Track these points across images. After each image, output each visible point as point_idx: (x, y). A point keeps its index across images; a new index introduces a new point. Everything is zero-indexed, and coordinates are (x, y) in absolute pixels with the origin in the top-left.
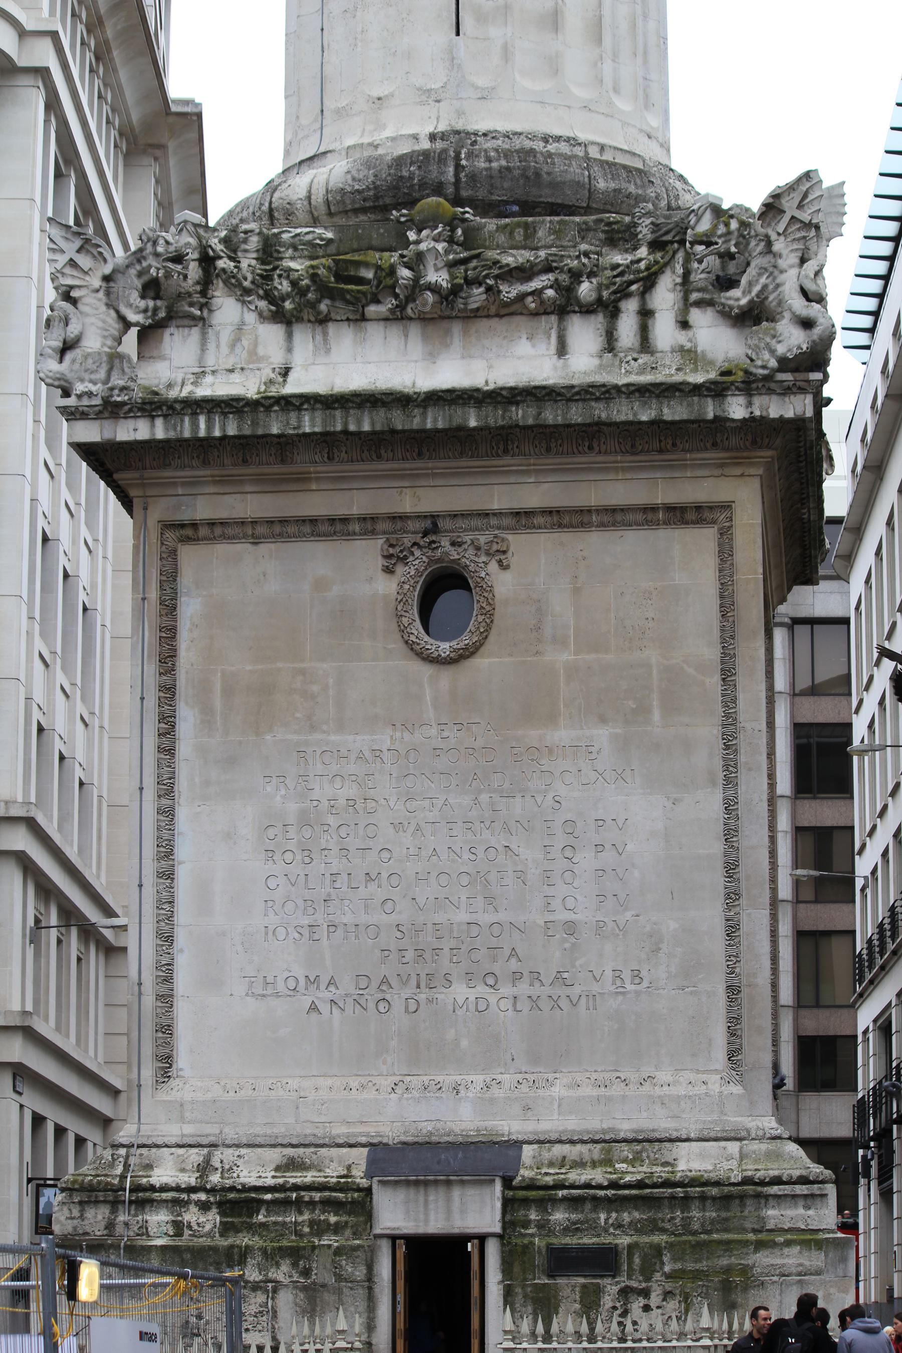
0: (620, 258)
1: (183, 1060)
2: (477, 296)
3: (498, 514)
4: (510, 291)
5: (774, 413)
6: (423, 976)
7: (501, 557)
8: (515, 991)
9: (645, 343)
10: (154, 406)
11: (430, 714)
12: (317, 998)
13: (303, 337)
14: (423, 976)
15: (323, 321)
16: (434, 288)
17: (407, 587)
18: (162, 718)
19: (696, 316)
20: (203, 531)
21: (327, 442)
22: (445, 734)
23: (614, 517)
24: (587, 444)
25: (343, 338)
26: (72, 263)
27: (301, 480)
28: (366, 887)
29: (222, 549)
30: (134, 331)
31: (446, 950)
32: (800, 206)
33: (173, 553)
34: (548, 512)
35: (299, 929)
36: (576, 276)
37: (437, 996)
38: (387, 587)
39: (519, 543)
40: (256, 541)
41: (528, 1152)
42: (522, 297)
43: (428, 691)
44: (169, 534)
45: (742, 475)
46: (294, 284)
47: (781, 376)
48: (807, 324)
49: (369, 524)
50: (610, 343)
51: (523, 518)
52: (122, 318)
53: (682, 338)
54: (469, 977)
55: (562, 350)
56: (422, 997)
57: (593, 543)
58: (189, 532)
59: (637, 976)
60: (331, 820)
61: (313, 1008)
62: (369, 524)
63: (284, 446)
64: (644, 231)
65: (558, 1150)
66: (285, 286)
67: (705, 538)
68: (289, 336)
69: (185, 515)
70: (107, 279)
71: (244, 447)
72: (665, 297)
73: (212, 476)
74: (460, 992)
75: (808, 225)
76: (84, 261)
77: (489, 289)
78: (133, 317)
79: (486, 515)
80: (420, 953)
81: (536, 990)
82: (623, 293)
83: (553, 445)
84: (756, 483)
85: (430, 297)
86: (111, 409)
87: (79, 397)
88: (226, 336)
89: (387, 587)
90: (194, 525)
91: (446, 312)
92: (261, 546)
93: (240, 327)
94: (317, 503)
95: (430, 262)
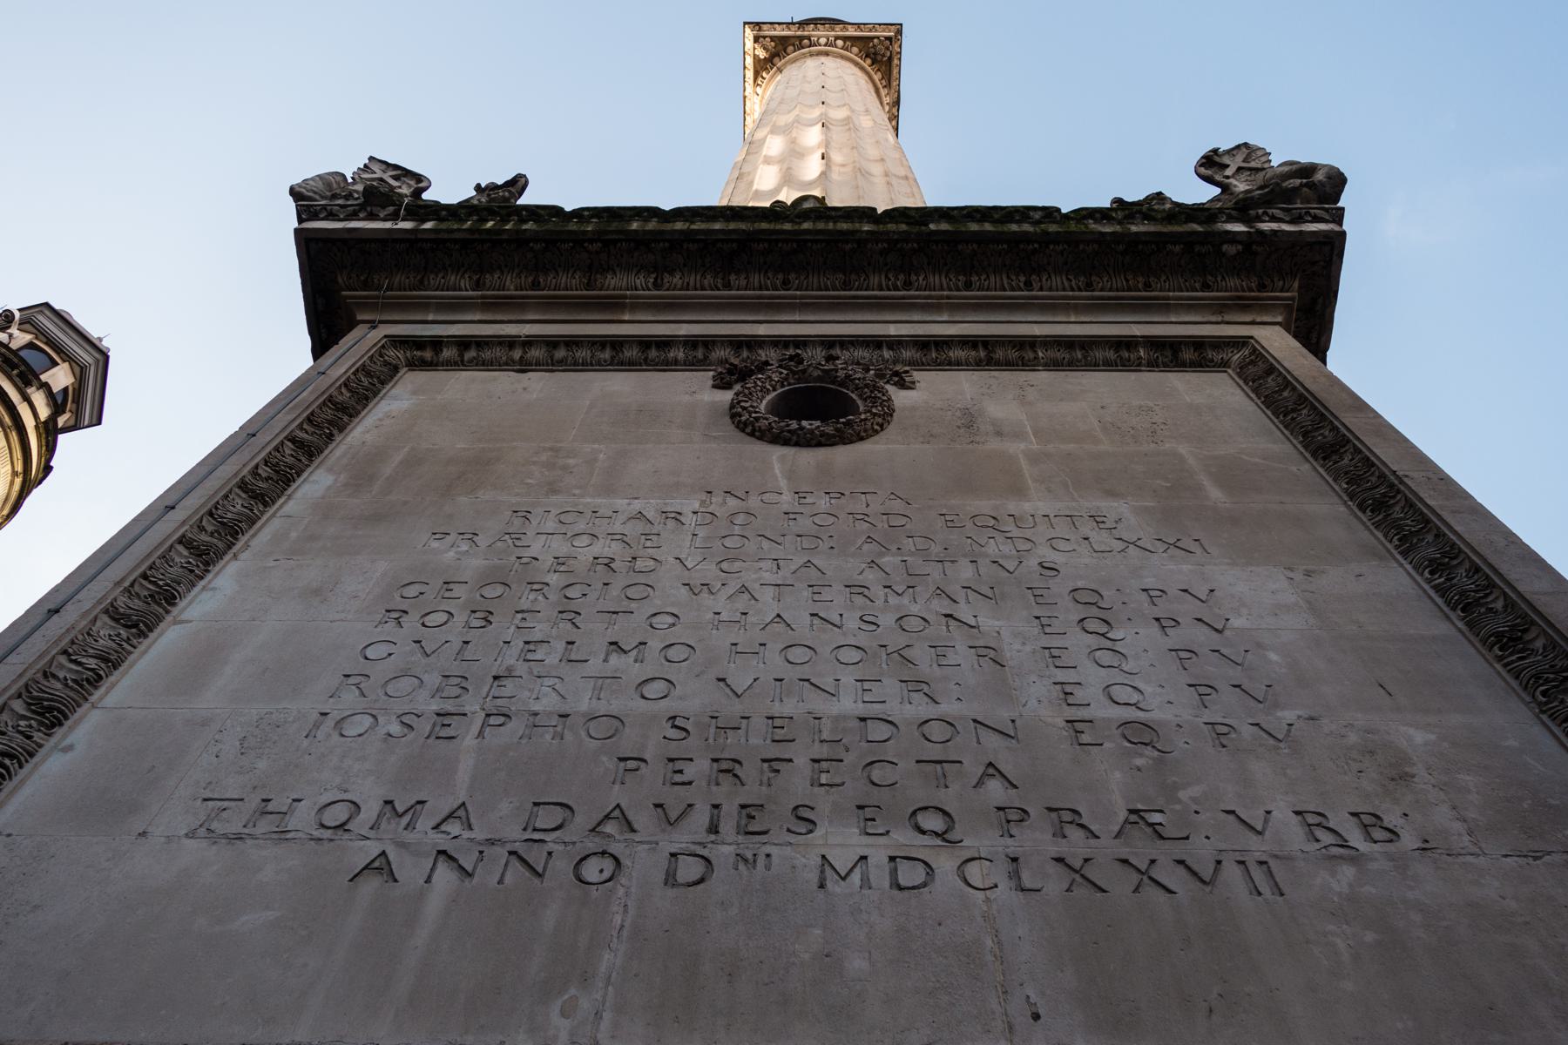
3: (895, 343)
6: (730, 809)
8: (1012, 846)
11: (783, 483)
12: (402, 845)
14: (730, 809)
20: (447, 353)
23: (1075, 354)
24: (1023, 279)
27: (613, 305)
28: (605, 660)
31: (801, 761)
35: (406, 719)
37: (768, 849)
44: (392, 354)
54: (867, 814)
56: (723, 852)
58: (428, 355)
59: (1370, 823)
60: (553, 579)
61: (381, 867)
62: (697, 353)
73: (483, 297)
80: (728, 769)
81: (1075, 845)
83: (975, 278)
92: (530, 374)
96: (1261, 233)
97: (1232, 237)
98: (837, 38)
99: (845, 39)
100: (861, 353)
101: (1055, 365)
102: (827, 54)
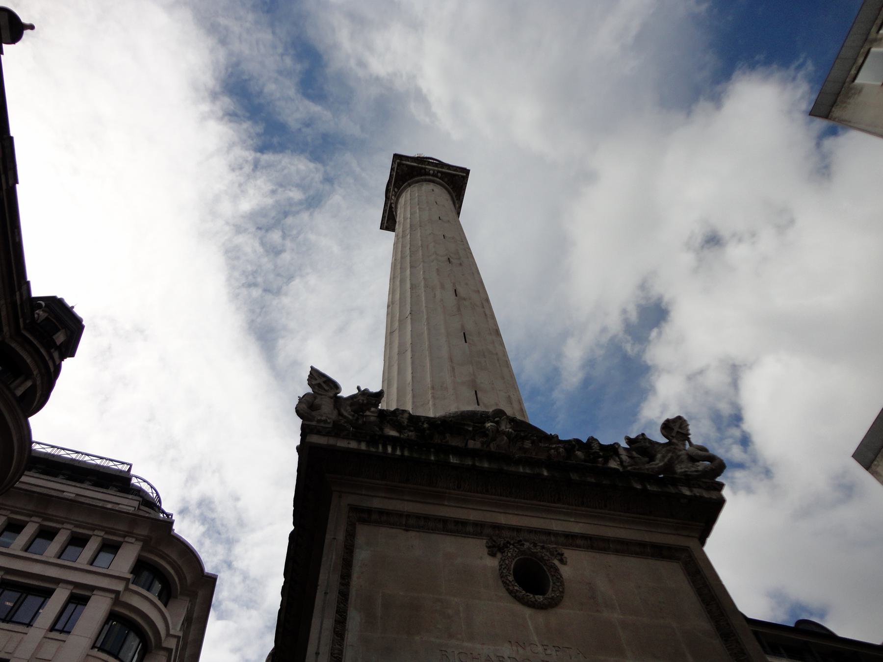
16: (508, 435)
17: (507, 562)
22: (549, 652)
23: (624, 547)
29: (384, 530)
32: (680, 428)
34: (584, 537)
39: (568, 553)
40: (407, 528)
43: (530, 623)
45: (688, 536)
51: (572, 540)
62: (477, 529)
79: (548, 533)
87: (319, 421)
89: (492, 563)
90: (369, 511)
96: (695, 496)
97: (685, 496)
98: (439, 172)
99: (442, 173)
100: (544, 538)
101: (617, 552)
102: (433, 182)
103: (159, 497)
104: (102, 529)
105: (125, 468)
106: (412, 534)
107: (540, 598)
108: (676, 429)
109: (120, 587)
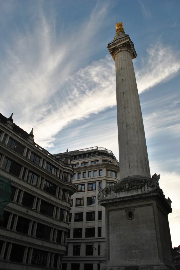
0: (142, 184)
1: (110, 258)
2: (130, 188)
3: (134, 206)
4: (133, 188)
5: (155, 195)
7: (134, 210)
9: (145, 190)
10: (106, 200)
13: (118, 193)
15: (119, 192)
16: (127, 188)
18: (108, 227)
19: (149, 188)
20: (111, 210)
21: (119, 202)
23: (143, 206)
25: (121, 193)
26: (100, 190)
30: (105, 195)
32: (155, 177)
33: (109, 212)
34: (138, 206)
36: (138, 186)
38: (125, 214)
41: (140, 267)
42: (134, 188)
46: (116, 189)
47: (155, 191)
48: (157, 186)
49: (123, 209)
50: (142, 191)
51: (136, 207)
52: (104, 194)
53: (148, 190)
55: (138, 192)
57: (142, 208)
59: (149, 249)
61: (121, 253)
62: (123, 209)
63: (116, 202)
64: (144, 181)
65: (143, 267)
66: (116, 190)
67: (152, 206)
68: (117, 194)
69: (109, 209)
70: (102, 190)
71: (113, 203)
72: (146, 186)
74: (134, 251)
75: (156, 178)
76: (101, 189)
77: (131, 188)
78: (104, 193)
82: (142, 187)
84: (155, 201)
85: (127, 189)
86: (102, 201)
88: (112, 194)
89: (125, 214)
90: (110, 210)
91: (128, 190)
93: (113, 194)
94: (119, 207)
95: (126, 186)
98: (121, 45)
103: (106, 149)
104: (98, 168)
105: (96, 148)
106: (116, 211)
107: (130, 219)
108: (154, 177)
109: (106, 178)
